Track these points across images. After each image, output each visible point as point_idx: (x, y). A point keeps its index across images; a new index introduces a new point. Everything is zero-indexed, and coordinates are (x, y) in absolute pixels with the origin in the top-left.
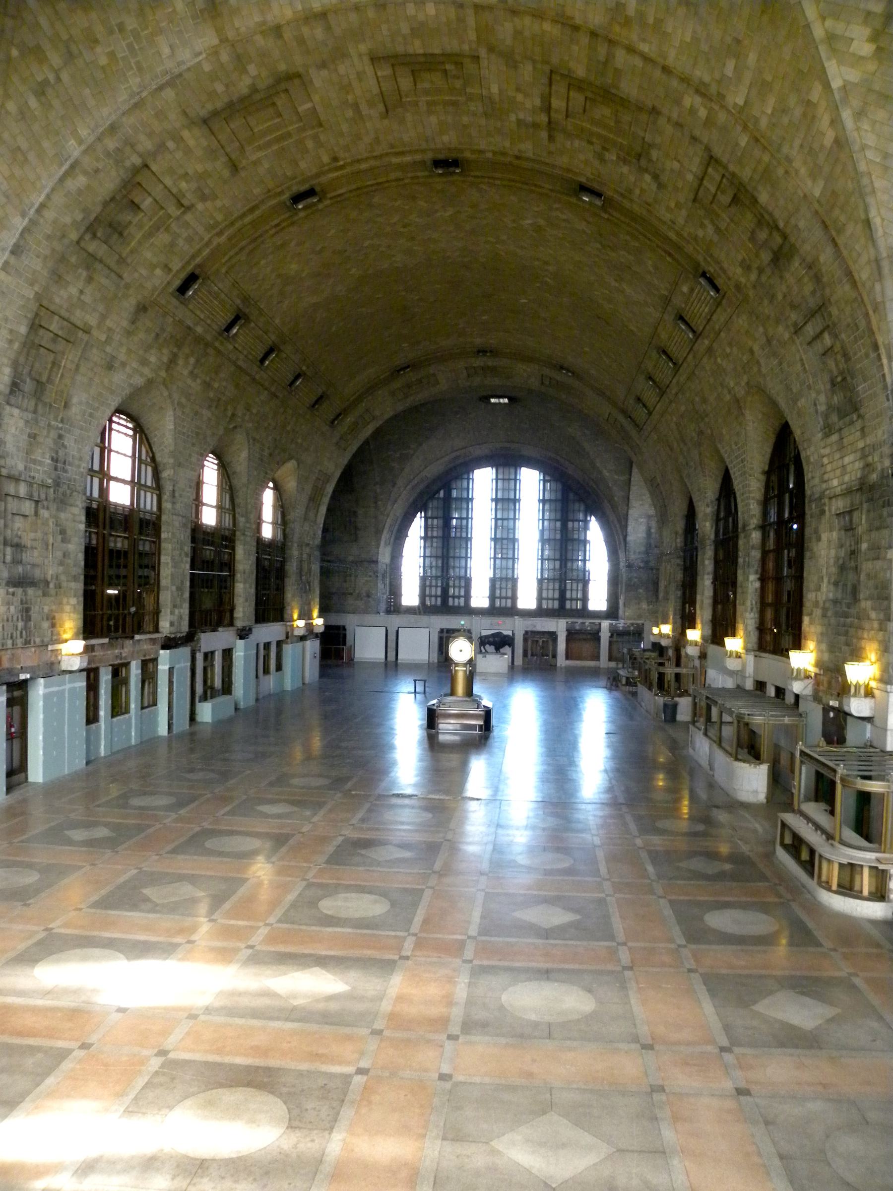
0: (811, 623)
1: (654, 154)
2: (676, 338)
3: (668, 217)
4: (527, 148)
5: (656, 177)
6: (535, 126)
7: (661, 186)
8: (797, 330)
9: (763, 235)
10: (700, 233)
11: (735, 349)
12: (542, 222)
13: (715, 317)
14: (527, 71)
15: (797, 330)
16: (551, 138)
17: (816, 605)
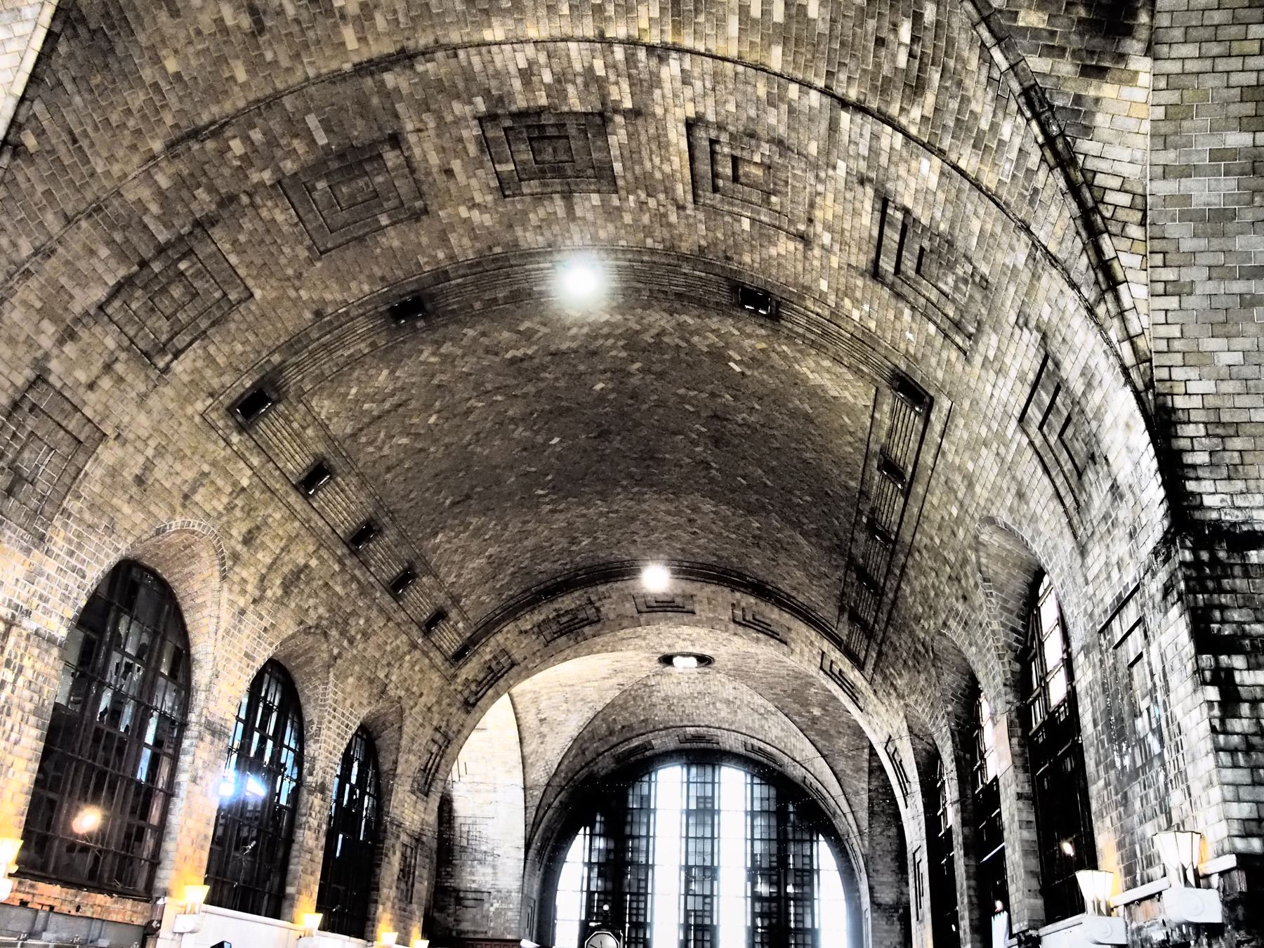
0: (384, 910)
1: (534, 637)
2: (420, 601)
3: (505, 630)
4: (602, 588)
5: (526, 632)
6: (600, 600)
7: (521, 632)
8: (437, 729)
9: (473, 687)
10: (488, 649)
11: (419, 676)
12: (574, 548)
13: (438, 653)
14: (612, 616)
15: (437, 729)
16: (589, 599)
17: (388, 899)
